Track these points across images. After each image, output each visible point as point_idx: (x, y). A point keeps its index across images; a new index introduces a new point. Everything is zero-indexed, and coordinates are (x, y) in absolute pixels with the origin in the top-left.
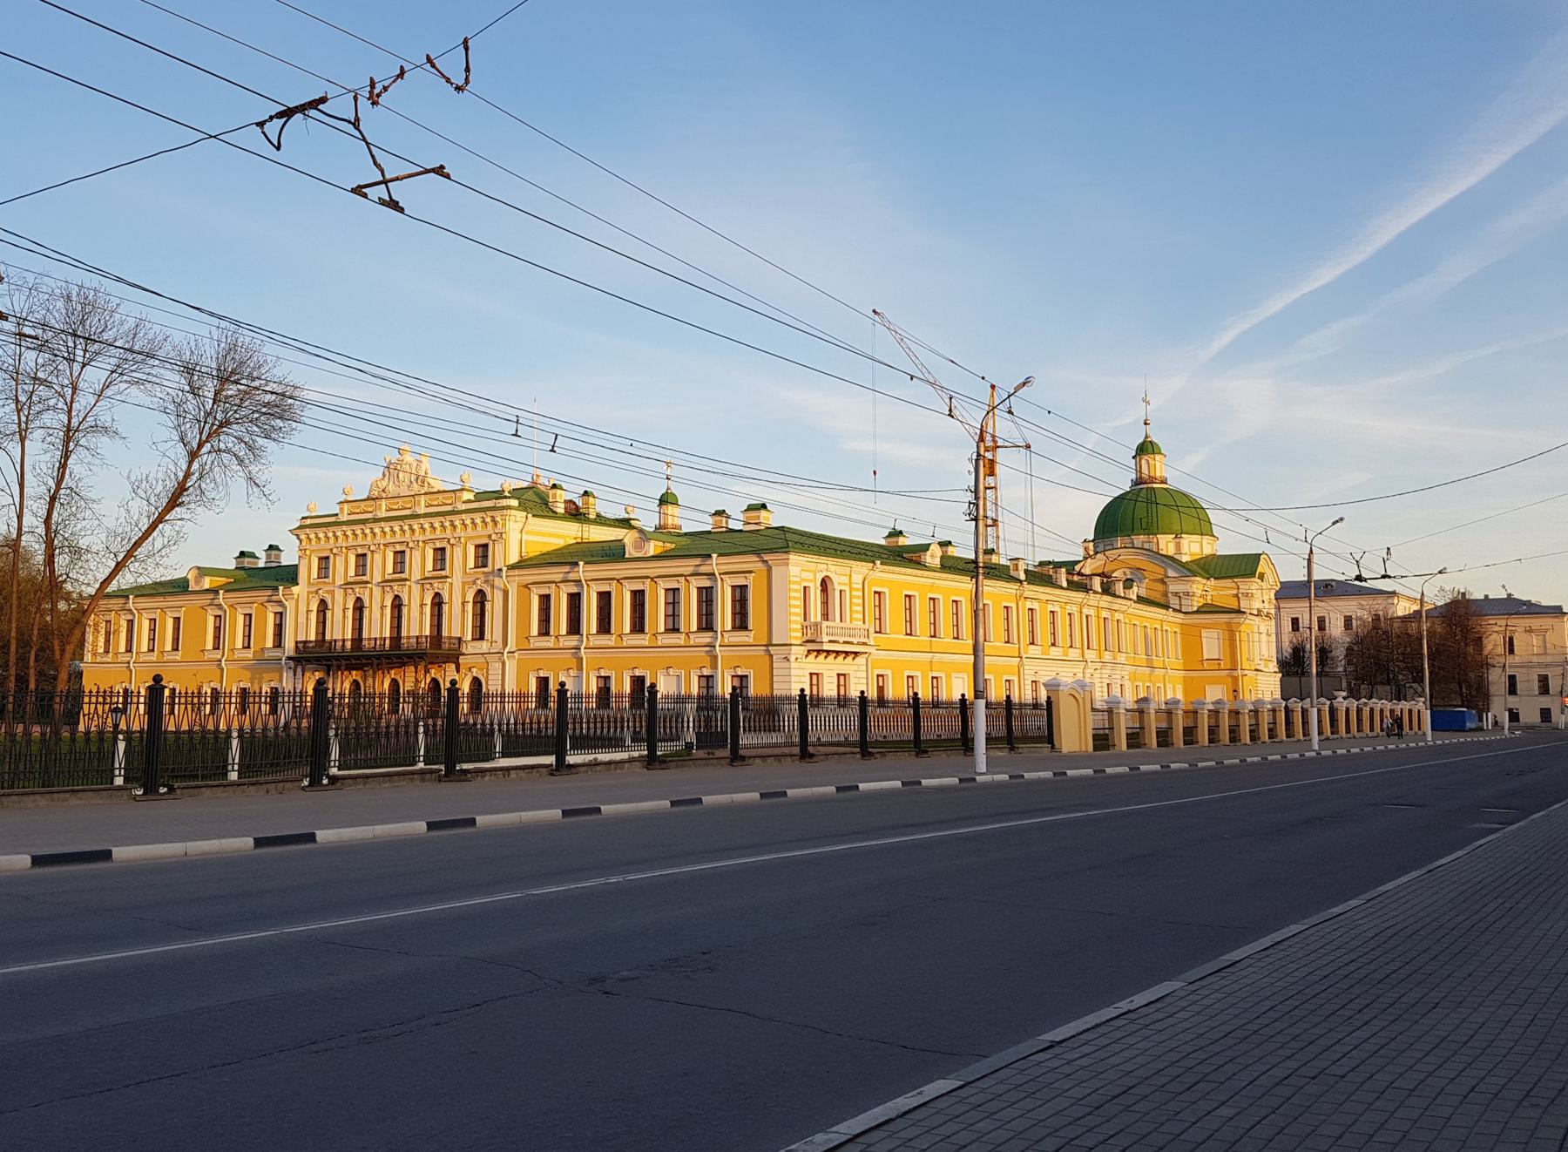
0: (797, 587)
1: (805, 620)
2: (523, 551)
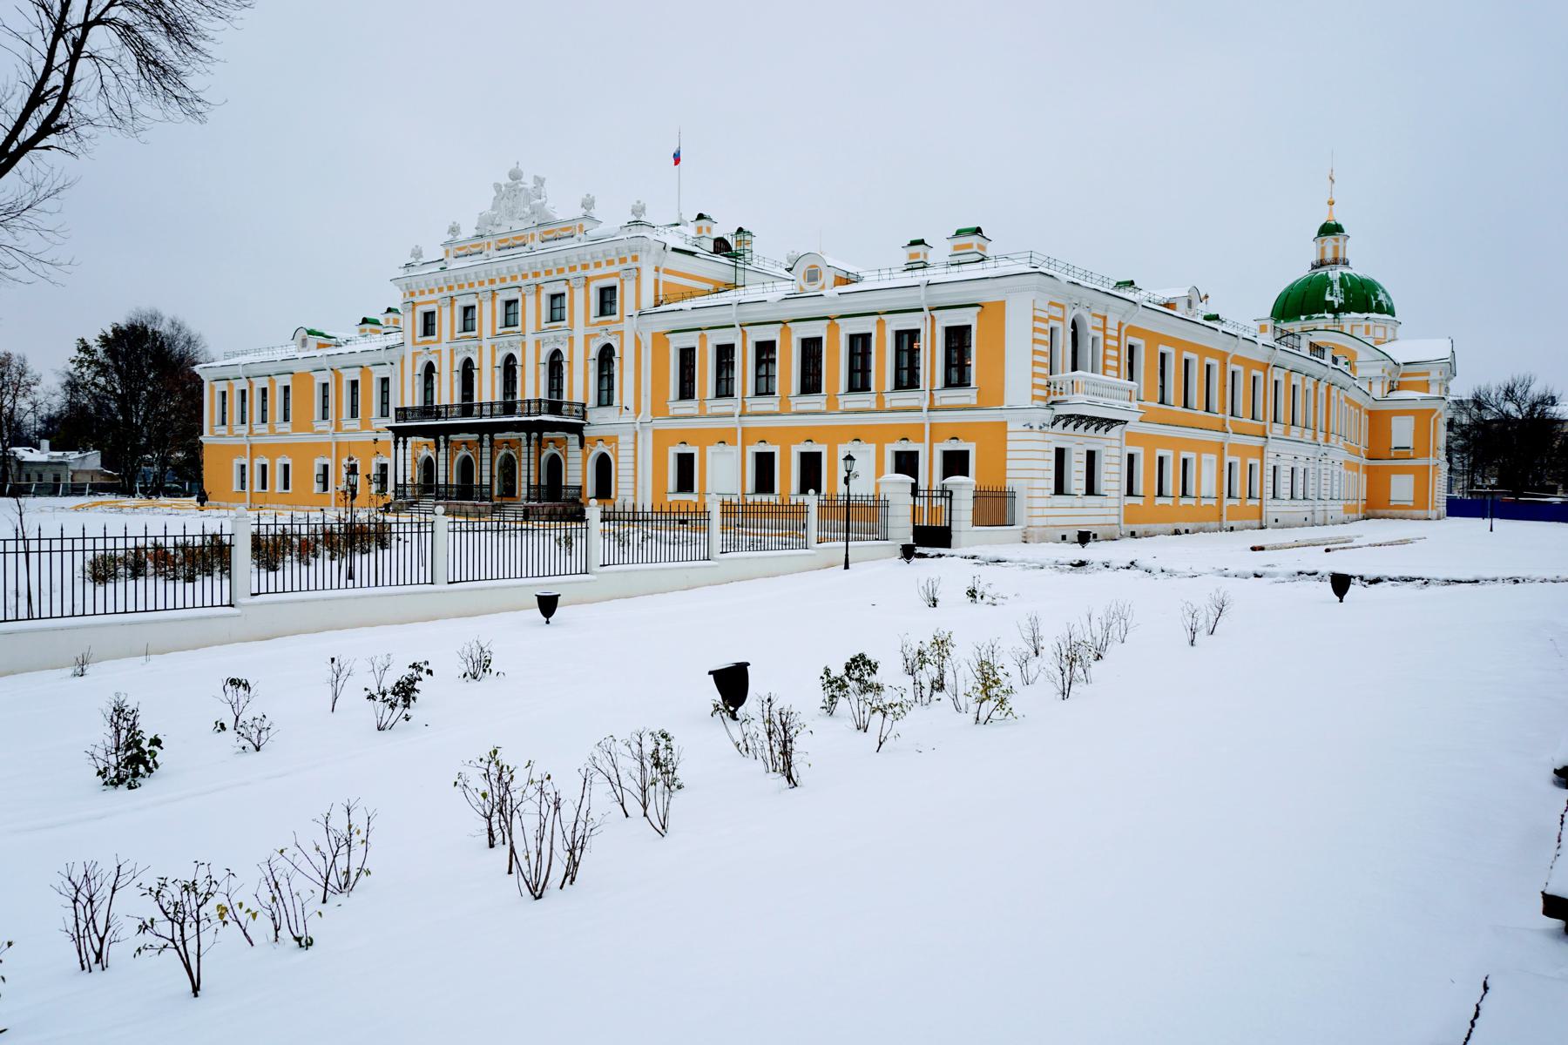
2: (661, 293)
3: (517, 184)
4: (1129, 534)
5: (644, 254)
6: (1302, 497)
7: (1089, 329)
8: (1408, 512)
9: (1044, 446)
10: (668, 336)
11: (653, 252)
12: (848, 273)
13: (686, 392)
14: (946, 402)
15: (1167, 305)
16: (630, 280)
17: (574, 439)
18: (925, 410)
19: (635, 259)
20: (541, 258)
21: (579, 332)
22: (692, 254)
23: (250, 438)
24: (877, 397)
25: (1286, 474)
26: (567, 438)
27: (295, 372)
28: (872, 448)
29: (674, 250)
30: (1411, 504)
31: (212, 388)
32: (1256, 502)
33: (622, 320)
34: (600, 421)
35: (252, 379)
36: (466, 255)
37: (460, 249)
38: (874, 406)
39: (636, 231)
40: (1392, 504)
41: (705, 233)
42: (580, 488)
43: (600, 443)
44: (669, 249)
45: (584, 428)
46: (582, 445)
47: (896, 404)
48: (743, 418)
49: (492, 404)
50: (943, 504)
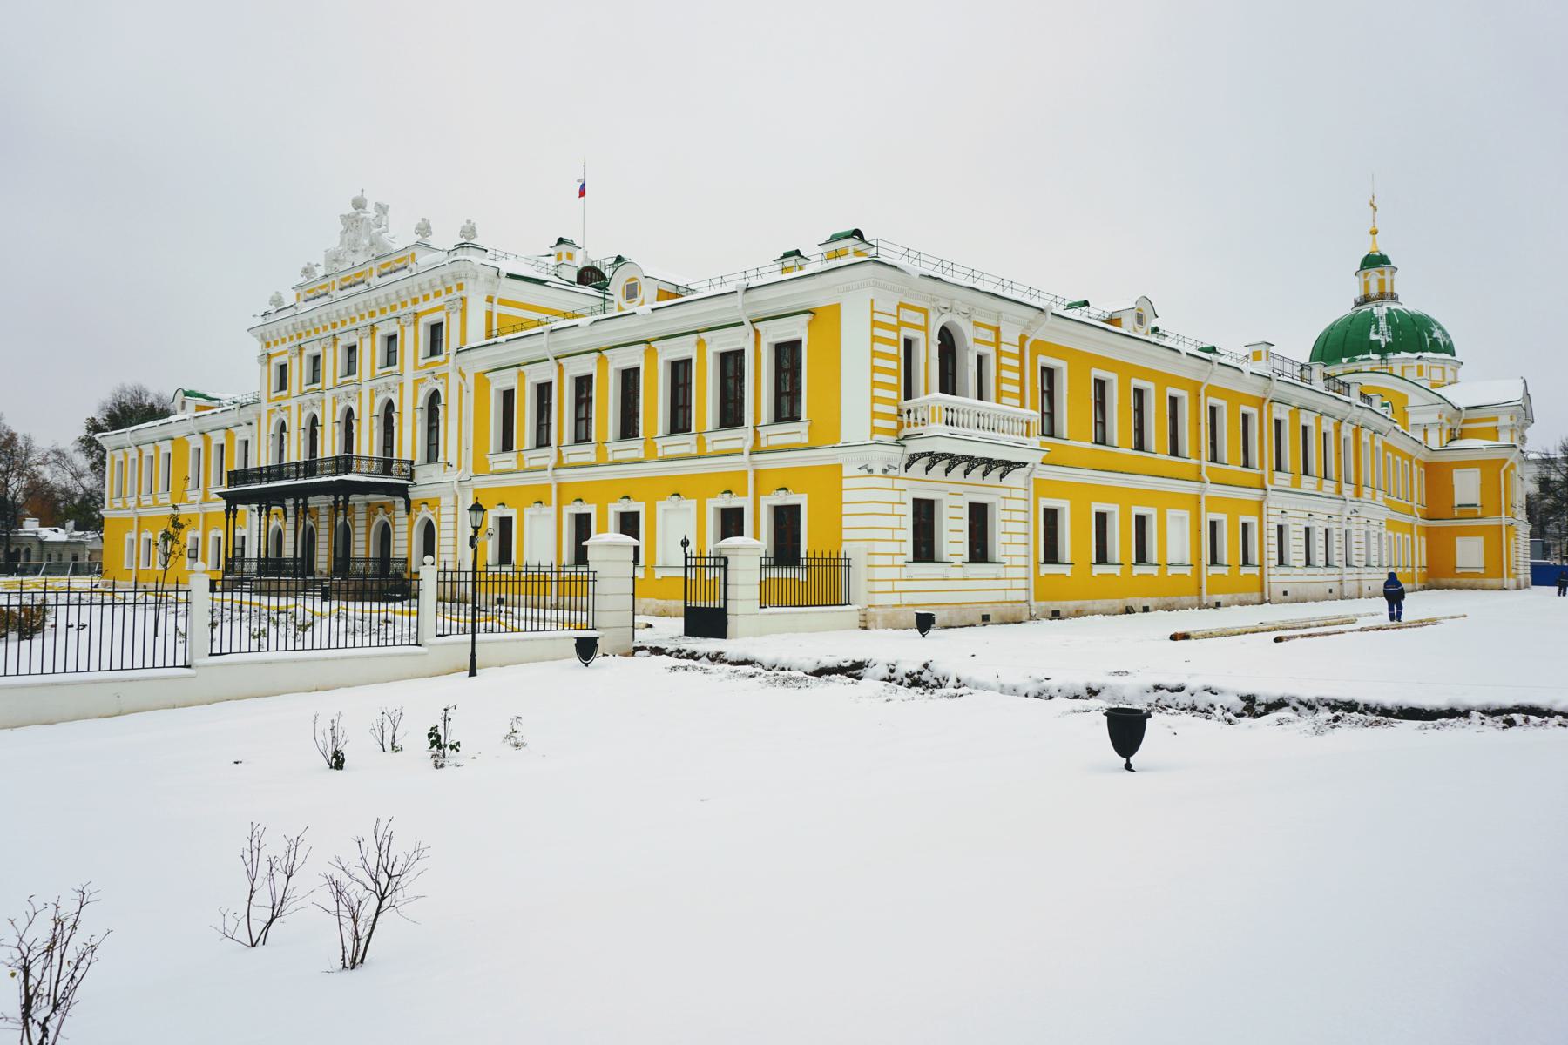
0: (892, 335)
1: (908, 396)
3: (358, 214)
4: (1142, 609)
5: (471, 282)
6: (1324, 563)
7: (970, 342)
8: (1479, 582)
9: (894, 496)
10: (486, 375)
11: (482, 278)
12: (677, 287)
13: (507, 445)
14: (774, 441)
15: (1110, 321)
16: (454, 312)
17: (400, 503)
18: (746, 453)
19: (460, 287)
20: (382, 292)
21: (409, 376)
22: (541, 282)
23: (138, 511)
24: (698, 439)
25: (1297, 535)
26: (394, 502)
27: (175, 437)
28: (692, 504)
29: (511, 276)
30: (1482, 571)
31: (113, 457)
32: (1256, 571)
33: (447, 361)
34: (428, 480)
35: (141, 447)
36: (314, 299)
37: (309, 292)
38: (694, 451)
39: (461, 255)
40: (1458, 571)
41: (564, 260)
42: (406, 559)
43: (424, 507)
44: (503, 275)
45: (409, 489)
46: (408, 510)
47: (719, 446)
48: (559, 472)
49: (297, 464)
50: (717, 575)
